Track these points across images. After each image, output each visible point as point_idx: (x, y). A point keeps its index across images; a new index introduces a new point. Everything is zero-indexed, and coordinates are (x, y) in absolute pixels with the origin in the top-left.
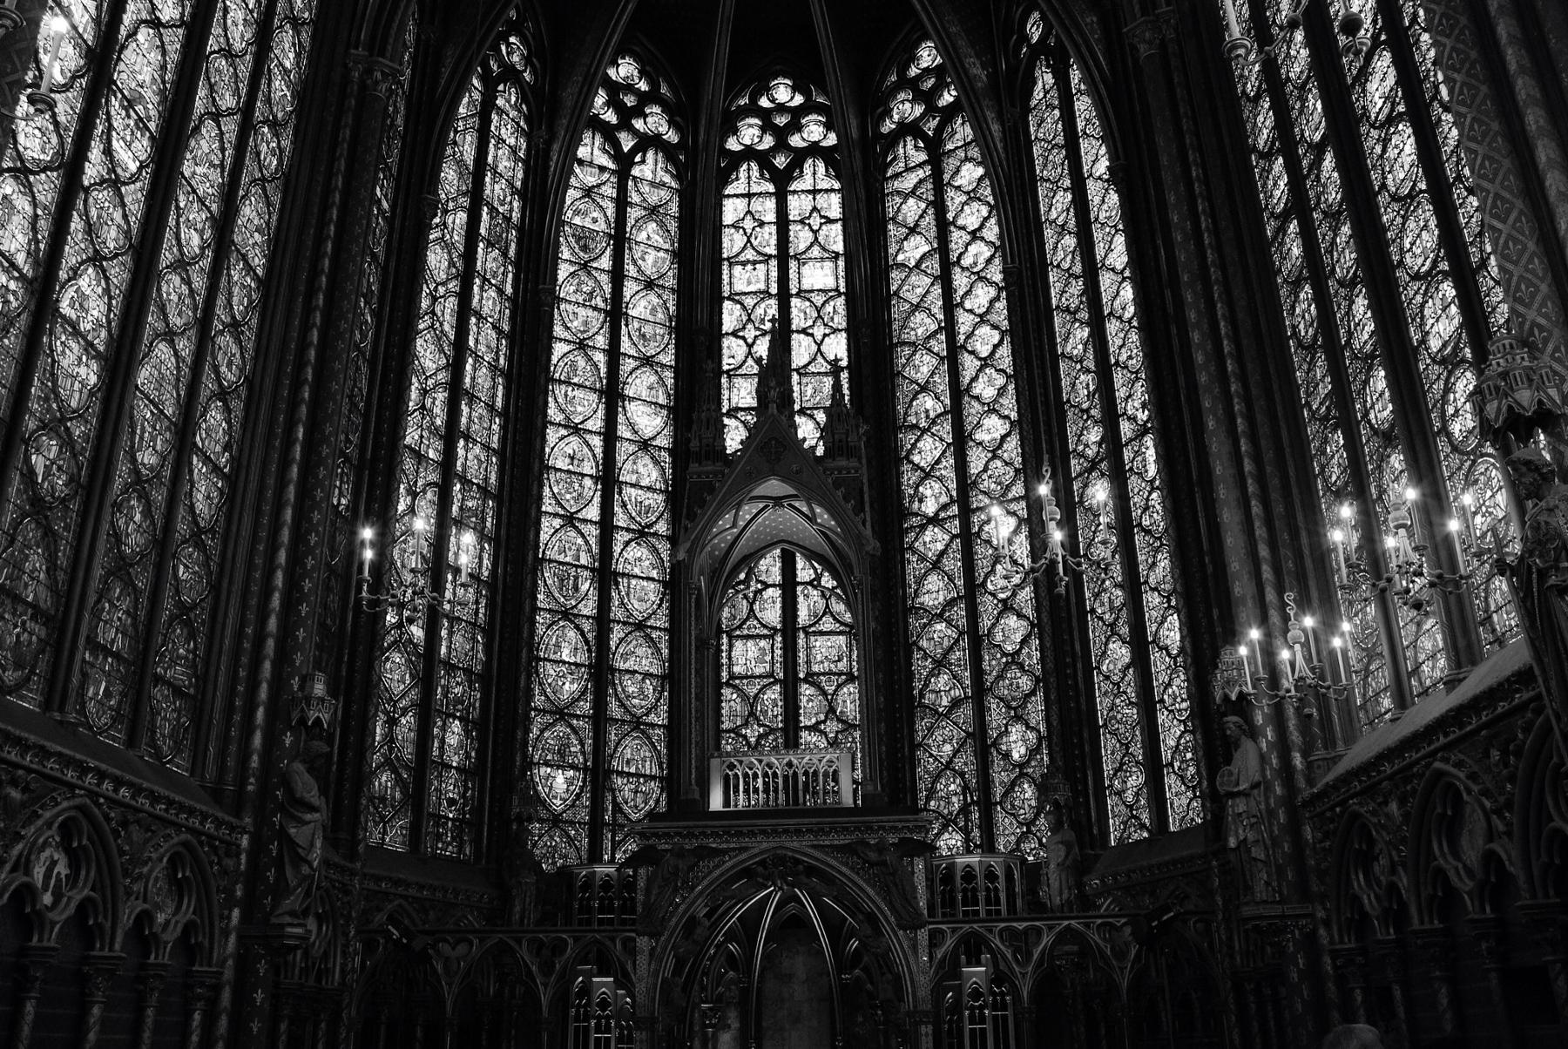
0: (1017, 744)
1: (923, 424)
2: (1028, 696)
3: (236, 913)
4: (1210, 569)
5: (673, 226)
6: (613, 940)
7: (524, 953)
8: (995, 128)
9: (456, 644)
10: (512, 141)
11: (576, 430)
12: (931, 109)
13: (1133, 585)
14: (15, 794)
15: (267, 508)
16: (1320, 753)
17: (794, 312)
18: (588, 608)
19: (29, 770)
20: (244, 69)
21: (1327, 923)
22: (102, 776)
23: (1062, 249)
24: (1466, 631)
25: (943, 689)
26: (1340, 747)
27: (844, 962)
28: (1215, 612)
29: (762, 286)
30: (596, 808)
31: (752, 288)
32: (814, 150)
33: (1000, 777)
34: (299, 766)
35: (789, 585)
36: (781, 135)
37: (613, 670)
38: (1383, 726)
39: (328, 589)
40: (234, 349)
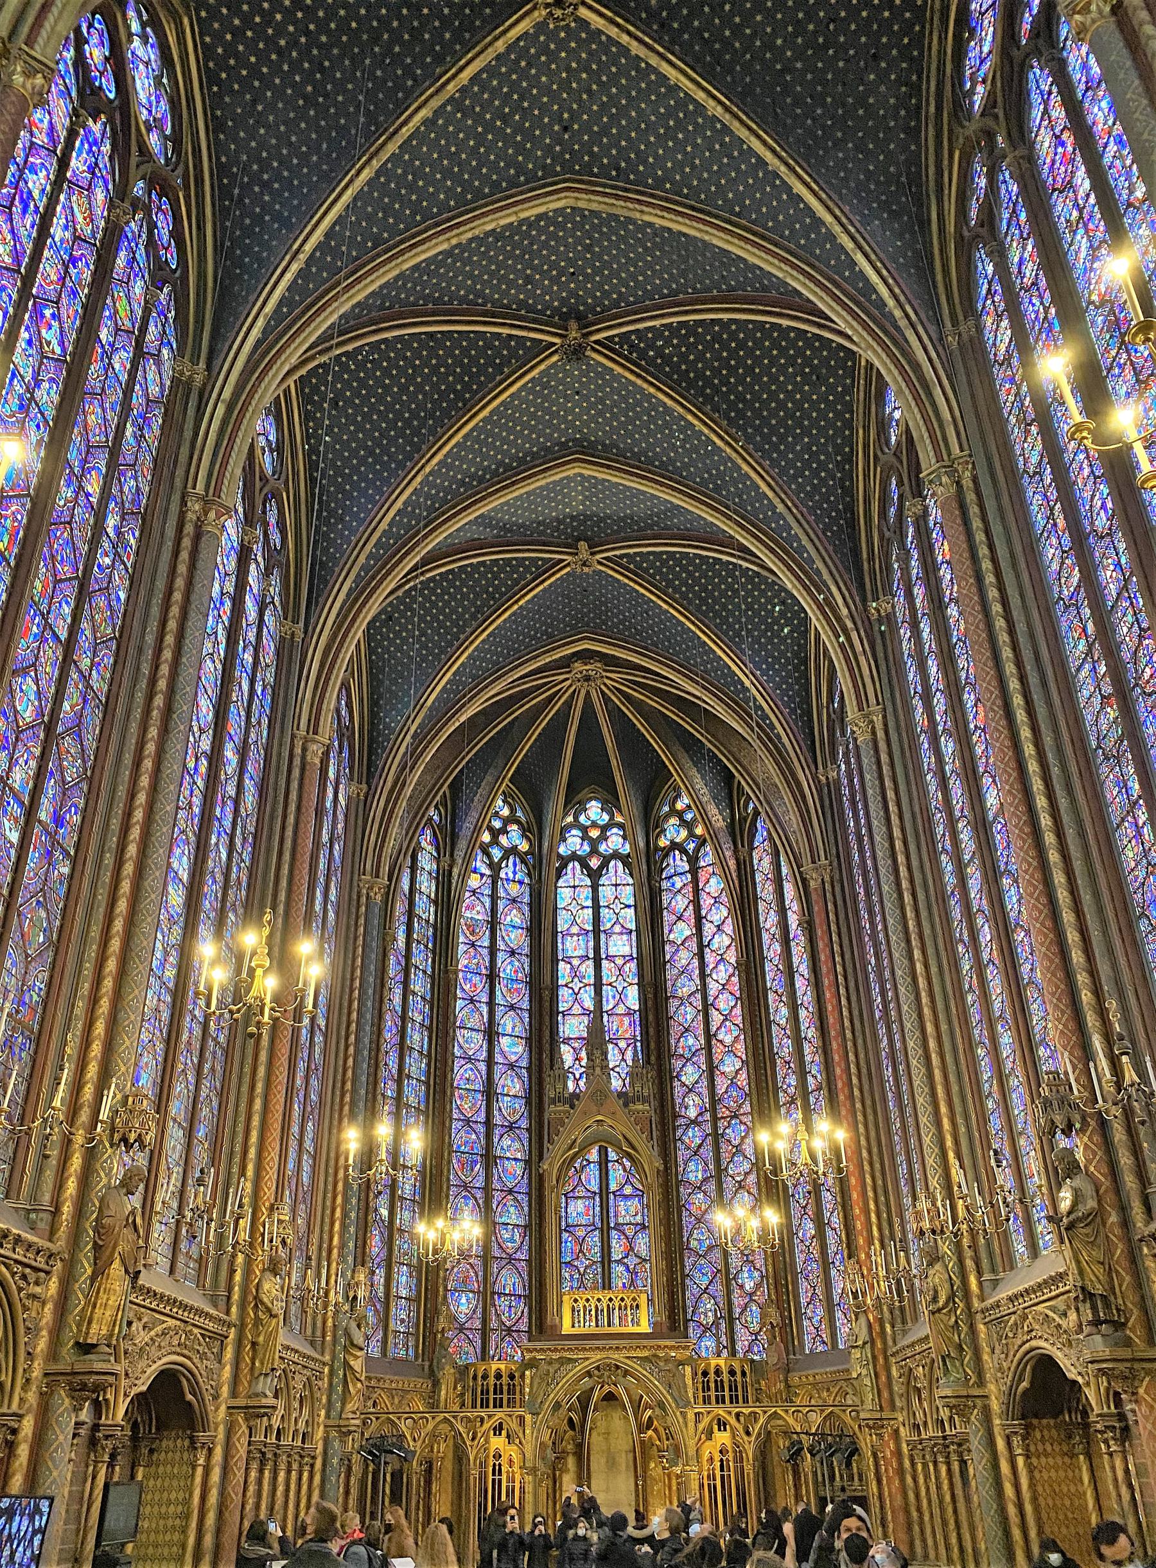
1: (688, 1055)
8: (732, 863)
10: (427, 868)
12: (691, 834)
15: (331, 1171)
16: (898, 1326)
17: (604, 972)
18: (480, 1182)
23: (772, 951)
29: (581, 952)
30: (485, 1321)
31: (576, 954)
32: (616, 855)
33: (738, 1301)
35: (603, 1163)
36: (594, 844)
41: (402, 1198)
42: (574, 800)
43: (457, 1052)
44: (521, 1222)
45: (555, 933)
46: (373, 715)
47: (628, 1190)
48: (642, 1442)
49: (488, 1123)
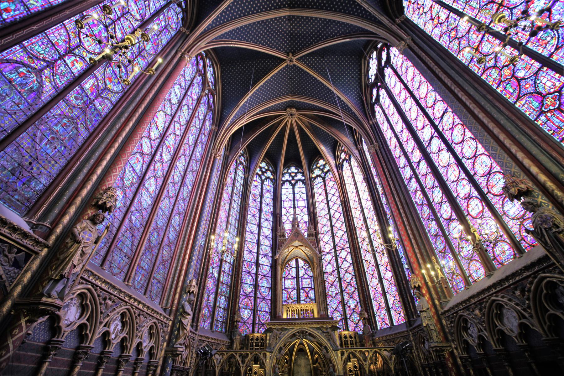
0: (352, 304)
1: (325, 233)
2: (353, 292)
3: (165, 344)
4: (397, 259)
5: (272, 194)
6: (260, 353)
7: (238, 357)
9: (224, 278)
11: (252, 233)
12: (323, 172)
13: (377, 266)
14: (110, 302)
16: (443, 300)
18: (254, 272)
19: (115, 296)
20: (192, 149)
21: (456, 349)
22: (135, 300)
23: (352, 195)
24: (489, 263)
25: (332, 291)
26: (448, 299)
27: (315, 361)
28: (400, 269)
32: (300, 180)
34: (187, 303)
35: (297, 267)
36: (293, 177)
37: (259, 286)
38: (459, 292)
39: (197, 262)
40: (183, 204)
41: (224, 272)
42: (287, 165)
43: (247, 229)
44: (269, 286)
45: (281, 201)
46: (222, 111)
47: (306, 276)
48: (314, 368)
49: (258, 253)
